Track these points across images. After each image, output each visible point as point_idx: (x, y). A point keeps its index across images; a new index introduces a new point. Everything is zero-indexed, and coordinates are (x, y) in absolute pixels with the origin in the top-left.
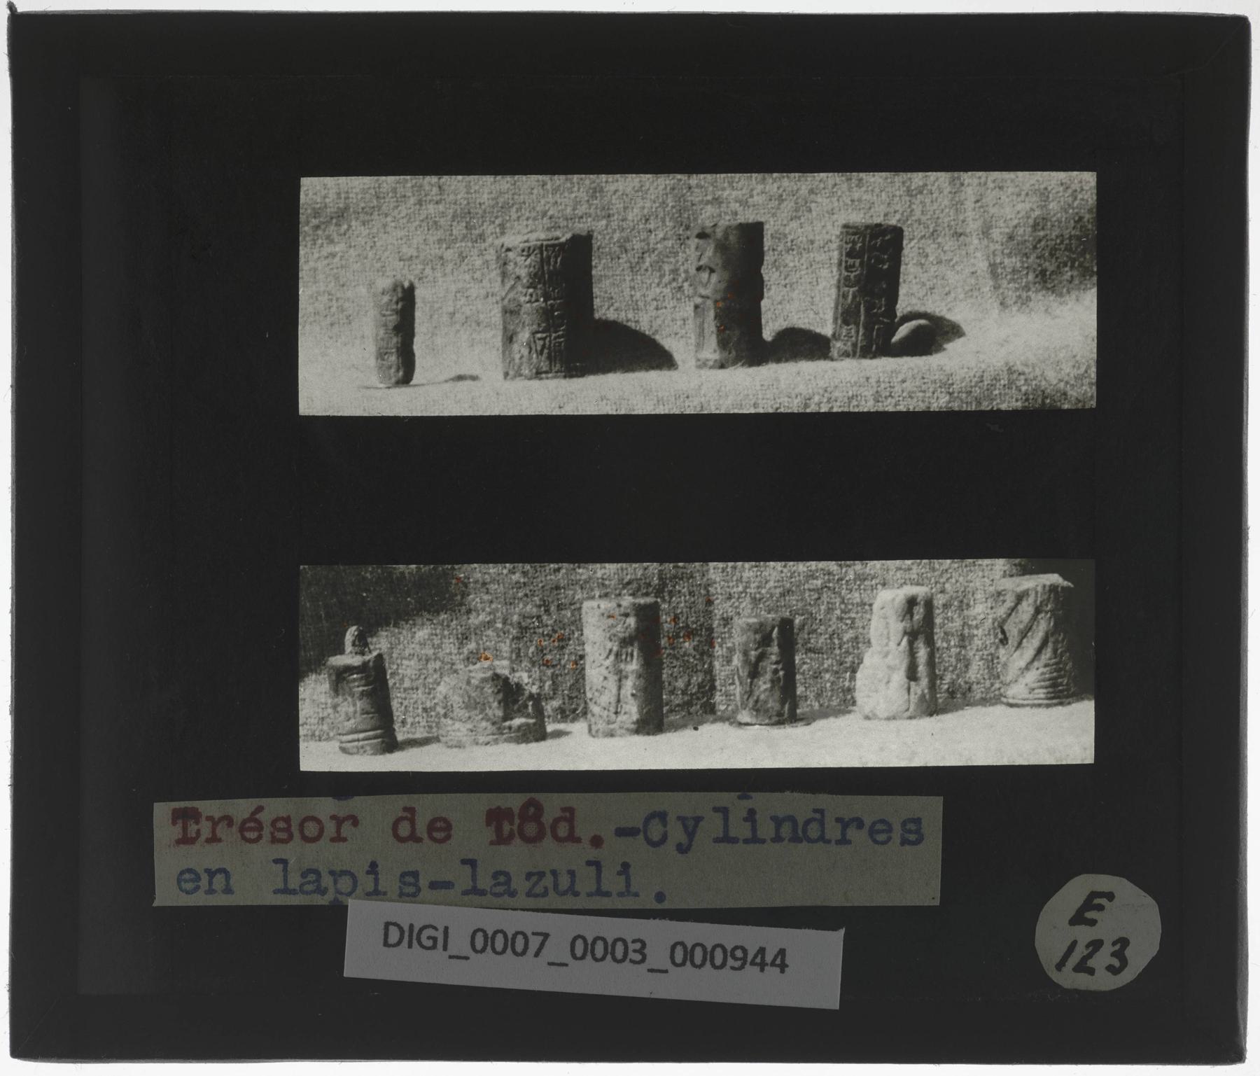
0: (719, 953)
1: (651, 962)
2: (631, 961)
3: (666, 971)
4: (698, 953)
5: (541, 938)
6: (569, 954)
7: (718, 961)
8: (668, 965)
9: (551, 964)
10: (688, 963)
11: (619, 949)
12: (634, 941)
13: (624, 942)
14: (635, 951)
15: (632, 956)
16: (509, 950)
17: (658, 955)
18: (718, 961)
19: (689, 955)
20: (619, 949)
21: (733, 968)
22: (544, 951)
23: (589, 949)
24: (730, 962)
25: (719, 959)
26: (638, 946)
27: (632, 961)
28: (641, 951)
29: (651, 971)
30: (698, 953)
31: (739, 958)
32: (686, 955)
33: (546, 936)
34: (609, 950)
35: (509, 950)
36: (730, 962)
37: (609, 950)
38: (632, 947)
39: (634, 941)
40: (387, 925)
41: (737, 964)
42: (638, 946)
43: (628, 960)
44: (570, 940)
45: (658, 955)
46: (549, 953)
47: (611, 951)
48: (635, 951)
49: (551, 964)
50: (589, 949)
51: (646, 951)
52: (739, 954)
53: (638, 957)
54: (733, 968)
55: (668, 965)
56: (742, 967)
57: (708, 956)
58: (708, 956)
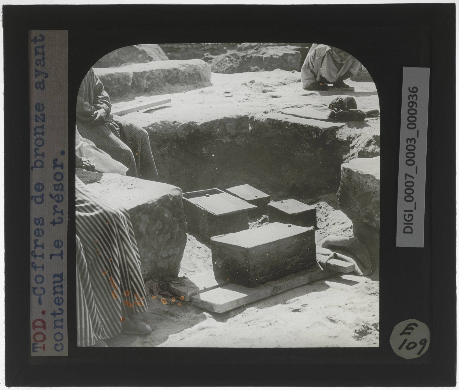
0: (411, 112)
1: (415, 137)
2: (414, 143)
3: (418, 131)
4: (411, 119)
5: (407, 176)
6: (413, 166)
7: (414, 112)
8: (416, 130)
9: (416, 173)
10: (415, 123)
11: (410, 148)
12: (407, 143)
13: (407, 147)
14: (411, 142)
15: (412, 143)
16: (412, 188)
17: (412, 134)
18: (414, 112)
19: (412, 123)
20: (410, 148)
21: (416, 107)
22: (412, 175)
23: (410, 159)
24: (414, 107)
25: (413, 112)
26: (409, 141)
27: (414, 143)
28: (411, 140)
29: (418, 137)
30: (411, 119)
31: (412, 105)
32: (412, 124)
33: (406, 175)
34: (410, 151)
35: (412, 188)
36: (414, 107)
37: (410, 151)
38: (409, 143)
39: (407, 143)
40: (404, 232)
41: (415, 105)
42: (409, 141)
43: (414, 145)
44: (408, 166)
45: (412, 134)
46: (413, 174)
47: (411, 151)
48: (411, 142)
49: (416, 173)
50: (410, 159)
51: (411, 138)
52: (411, 104)
53: (413, 141)
54: (416, 107)
55: (415, 130)
56: (415, 103)
57: (412, 115)
58: (412, 115)
